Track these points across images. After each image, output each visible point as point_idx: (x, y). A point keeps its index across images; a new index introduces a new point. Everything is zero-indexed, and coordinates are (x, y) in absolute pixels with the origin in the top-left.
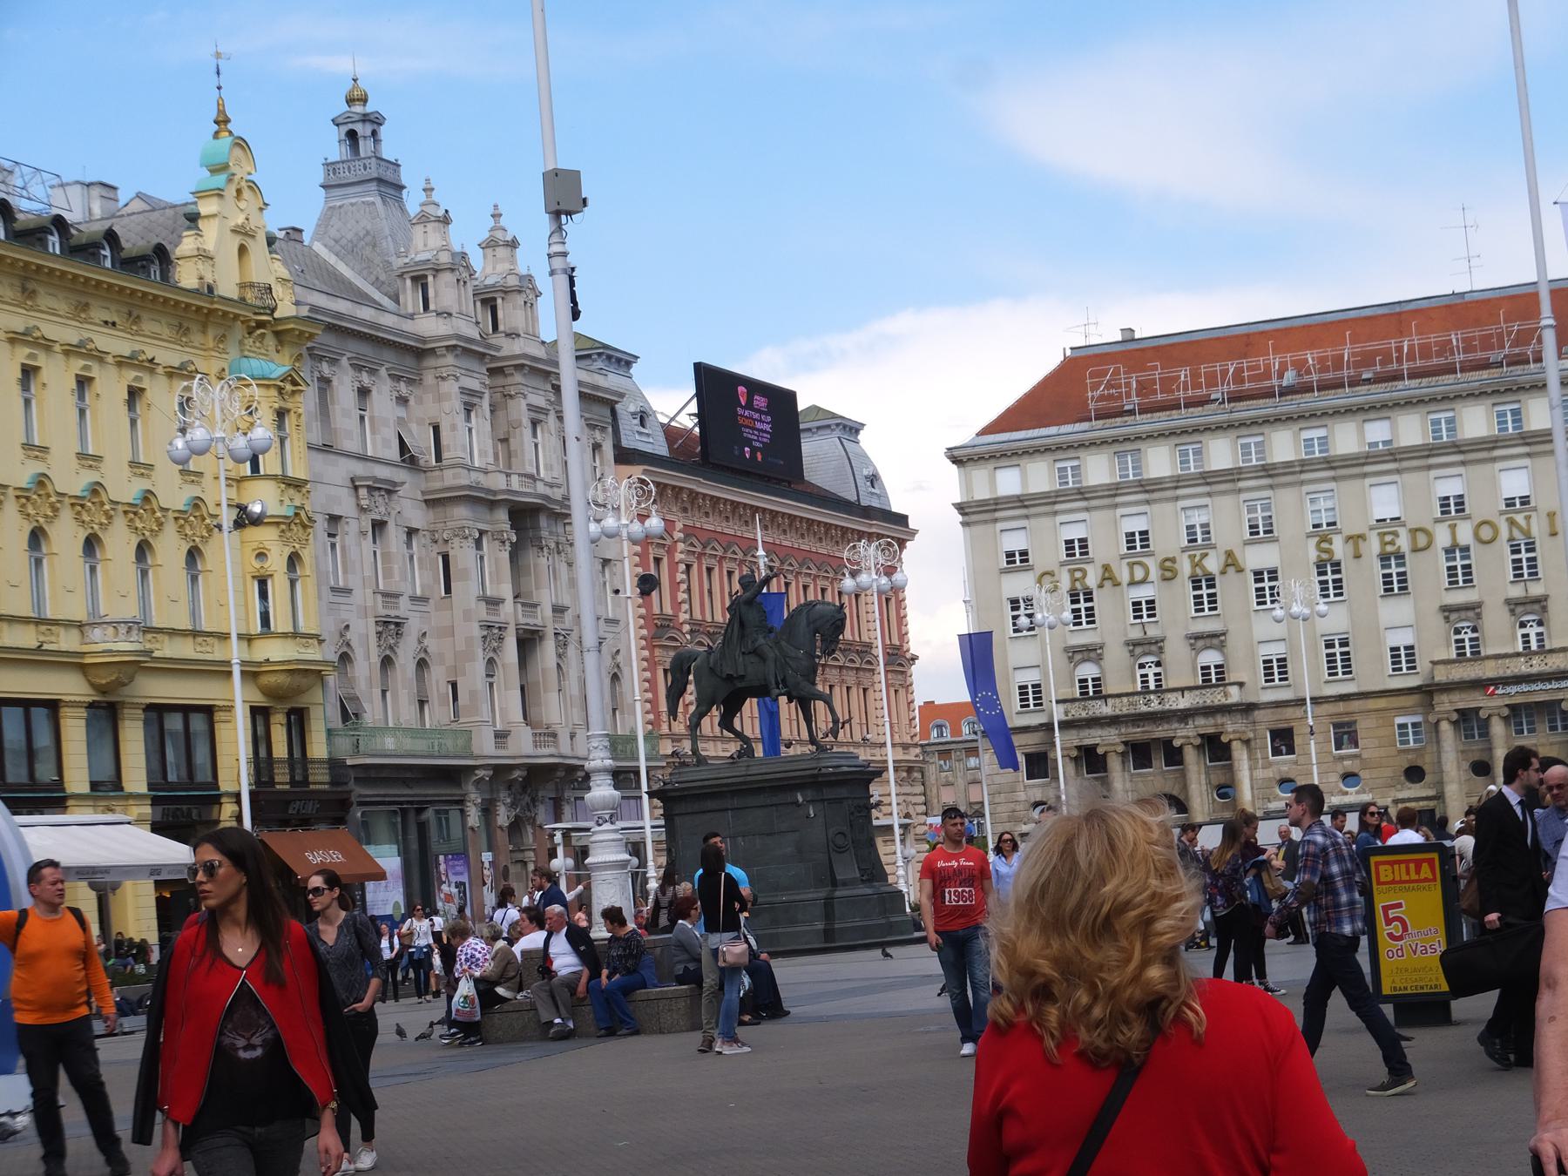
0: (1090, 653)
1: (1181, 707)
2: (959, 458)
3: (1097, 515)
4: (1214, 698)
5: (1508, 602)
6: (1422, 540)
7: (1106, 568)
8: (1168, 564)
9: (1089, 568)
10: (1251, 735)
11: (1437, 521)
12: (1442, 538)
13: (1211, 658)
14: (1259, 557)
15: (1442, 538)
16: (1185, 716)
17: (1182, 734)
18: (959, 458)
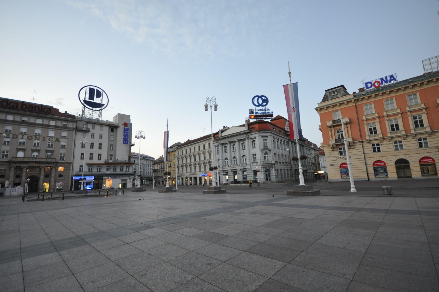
5: (32, 149)
6: (15, 136)
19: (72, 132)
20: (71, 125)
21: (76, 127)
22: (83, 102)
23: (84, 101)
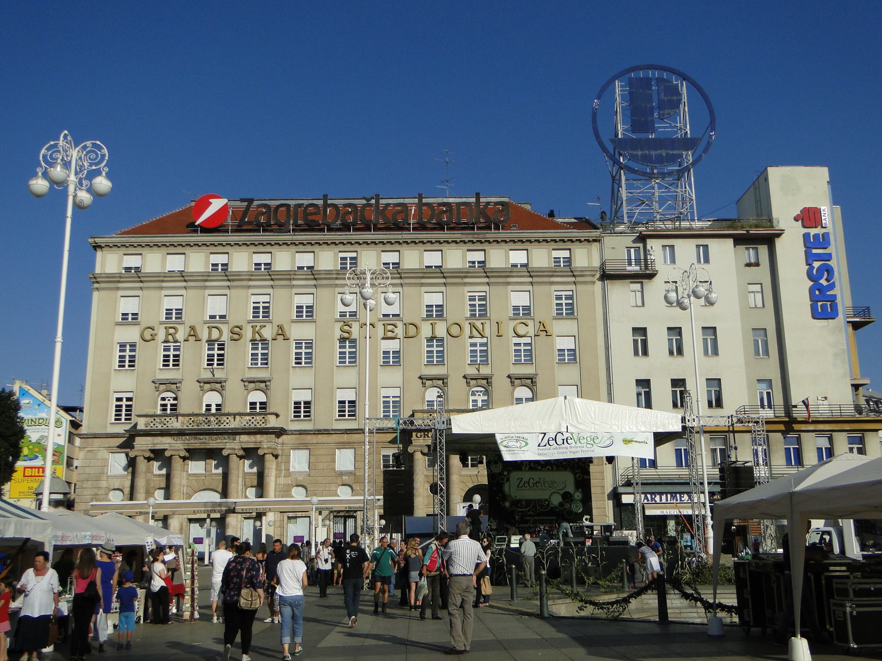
0: (172, 385)
1: (232, 426)
3: (192, 292)
4: (257, 422)
7: (192, 328)
8: (237, 330)
9: (181, 328)
10: (280, 452)
11: (423, 320)
12: (426, 330)
13: (258, 397)
14: (301, 331)
15: (426, 330)
16: (234, 433)
17: (231, 446)
19: (589, 287)
20: (585, 257)
21: (603, 264)
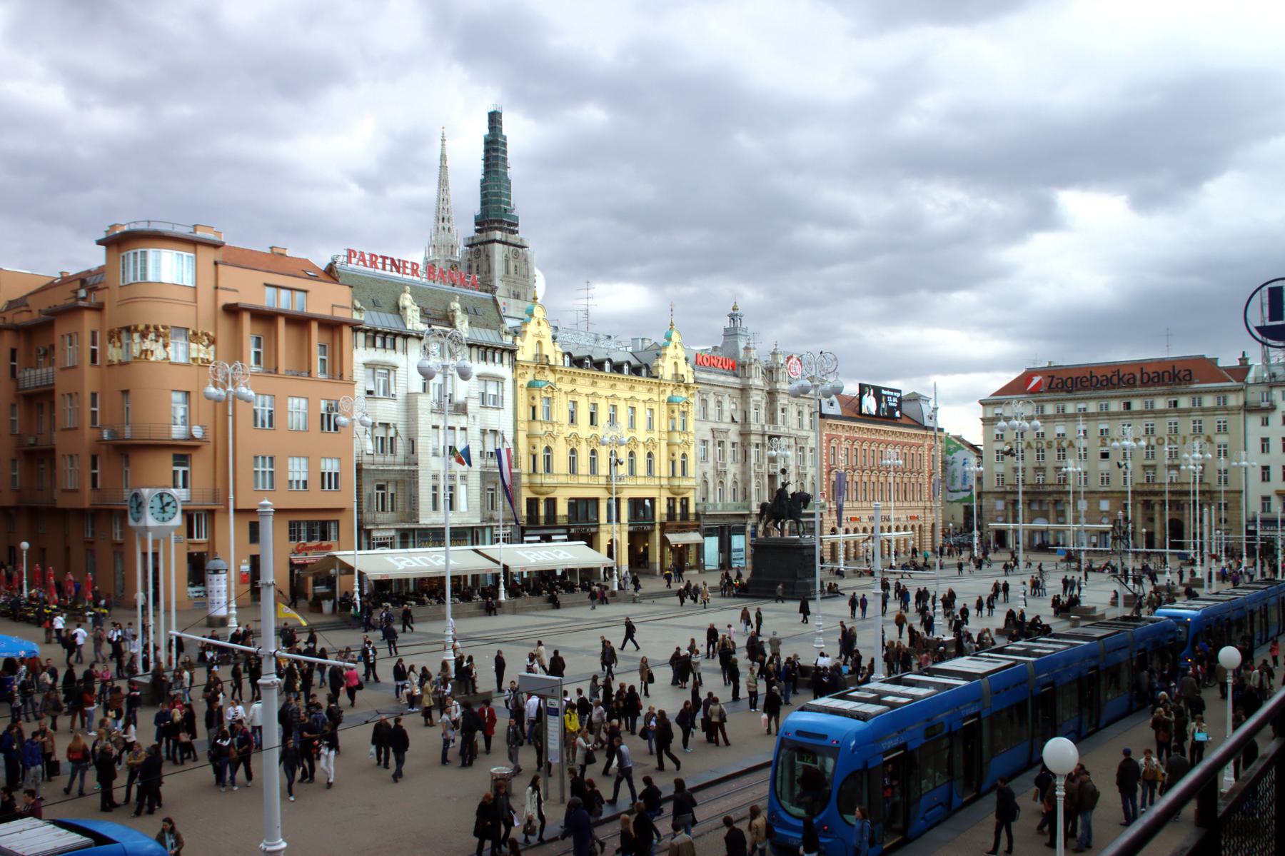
2: (984, 403)
16: (1050, 493)
18: (984, 403)
20: (1234, 400)
21: (1245, 403)
22: (1259, 336)
23: (1258, 328)
